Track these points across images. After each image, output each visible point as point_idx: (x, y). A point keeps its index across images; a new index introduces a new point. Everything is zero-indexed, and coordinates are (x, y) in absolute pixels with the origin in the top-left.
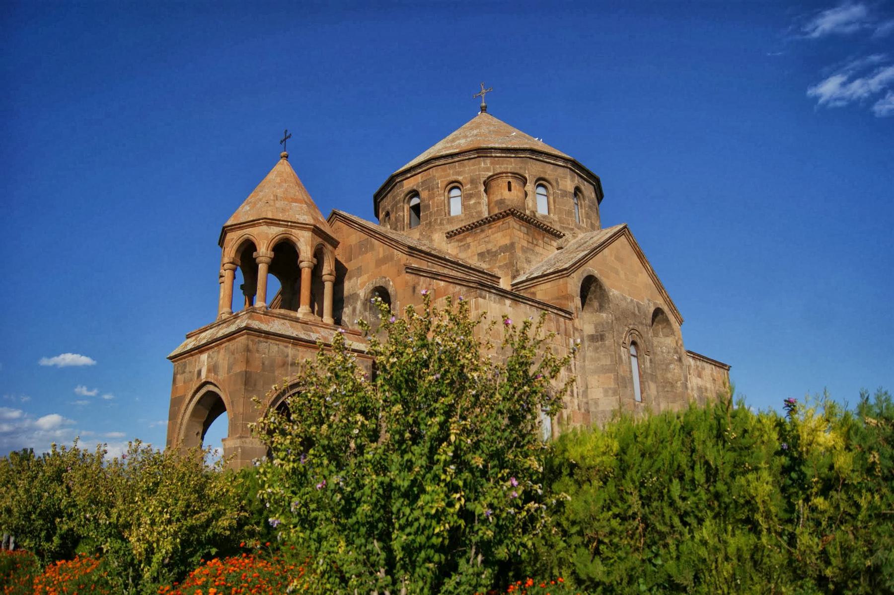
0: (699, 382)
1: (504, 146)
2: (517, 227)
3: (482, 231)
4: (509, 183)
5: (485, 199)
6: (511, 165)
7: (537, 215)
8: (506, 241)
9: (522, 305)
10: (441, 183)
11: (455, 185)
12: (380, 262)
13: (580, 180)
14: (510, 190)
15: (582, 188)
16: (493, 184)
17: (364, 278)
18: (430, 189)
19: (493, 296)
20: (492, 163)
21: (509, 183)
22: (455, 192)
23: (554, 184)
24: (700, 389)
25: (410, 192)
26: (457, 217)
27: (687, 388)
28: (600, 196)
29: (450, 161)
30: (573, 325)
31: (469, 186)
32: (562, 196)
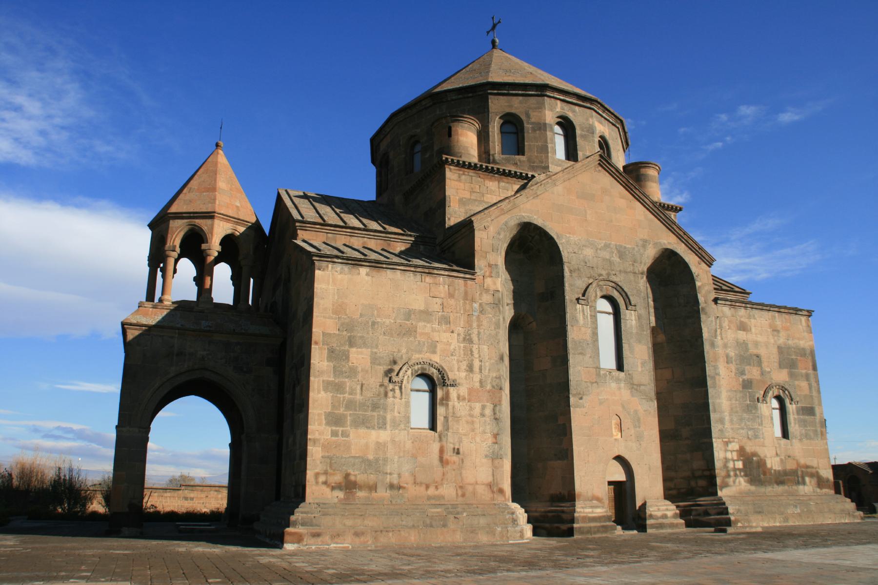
0: (742, 335)
4: (450, 129)
9: (389, 271)
11: (414, 141)
13: (567, 107)
15: (571, 116)
19: (339, 267)
22: (418, 148)
23: (523, 117)
24: (742, 345)
27: (713, 345)
28: (618, 122)
32: (534, 130)
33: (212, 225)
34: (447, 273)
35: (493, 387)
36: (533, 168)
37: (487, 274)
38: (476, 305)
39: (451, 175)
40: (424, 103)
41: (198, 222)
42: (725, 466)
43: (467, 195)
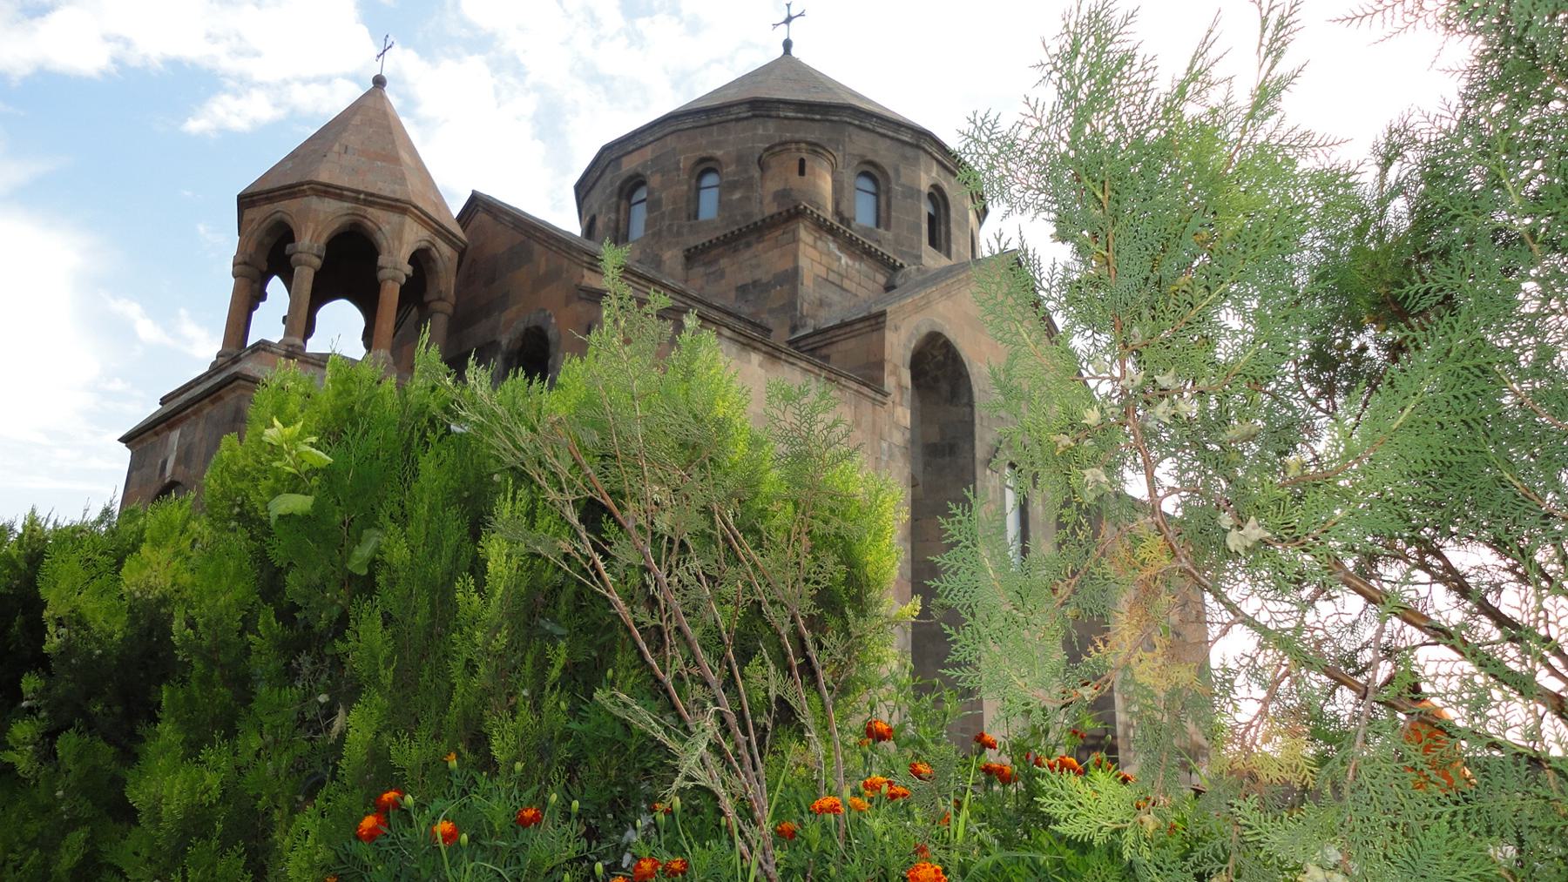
1: (802, 97)
3: (748, 245)
4: (802, 162)
6: (814, 133)
7: (853, 225)
8: (784, 265)
9: (787, 368)
10: (685, 161)
11: (707, 166)
13: (943, 173)
15: (946, 186)
16: (773, 162)
22: (711, 180)
23: (891, 173)
25: (631, 178)
26: (707, 222)
30: (891, 415)
31: (732, 168)
33: (402, 225)
34: (855, 386)
35: (901, 575)
36: (902, 254)
37: (897, 400)
38: (885, 445)
39: (805, 235)
40: (735, 110)
41: (372, 212)
42: (1126, 735)
43: (822, 271)
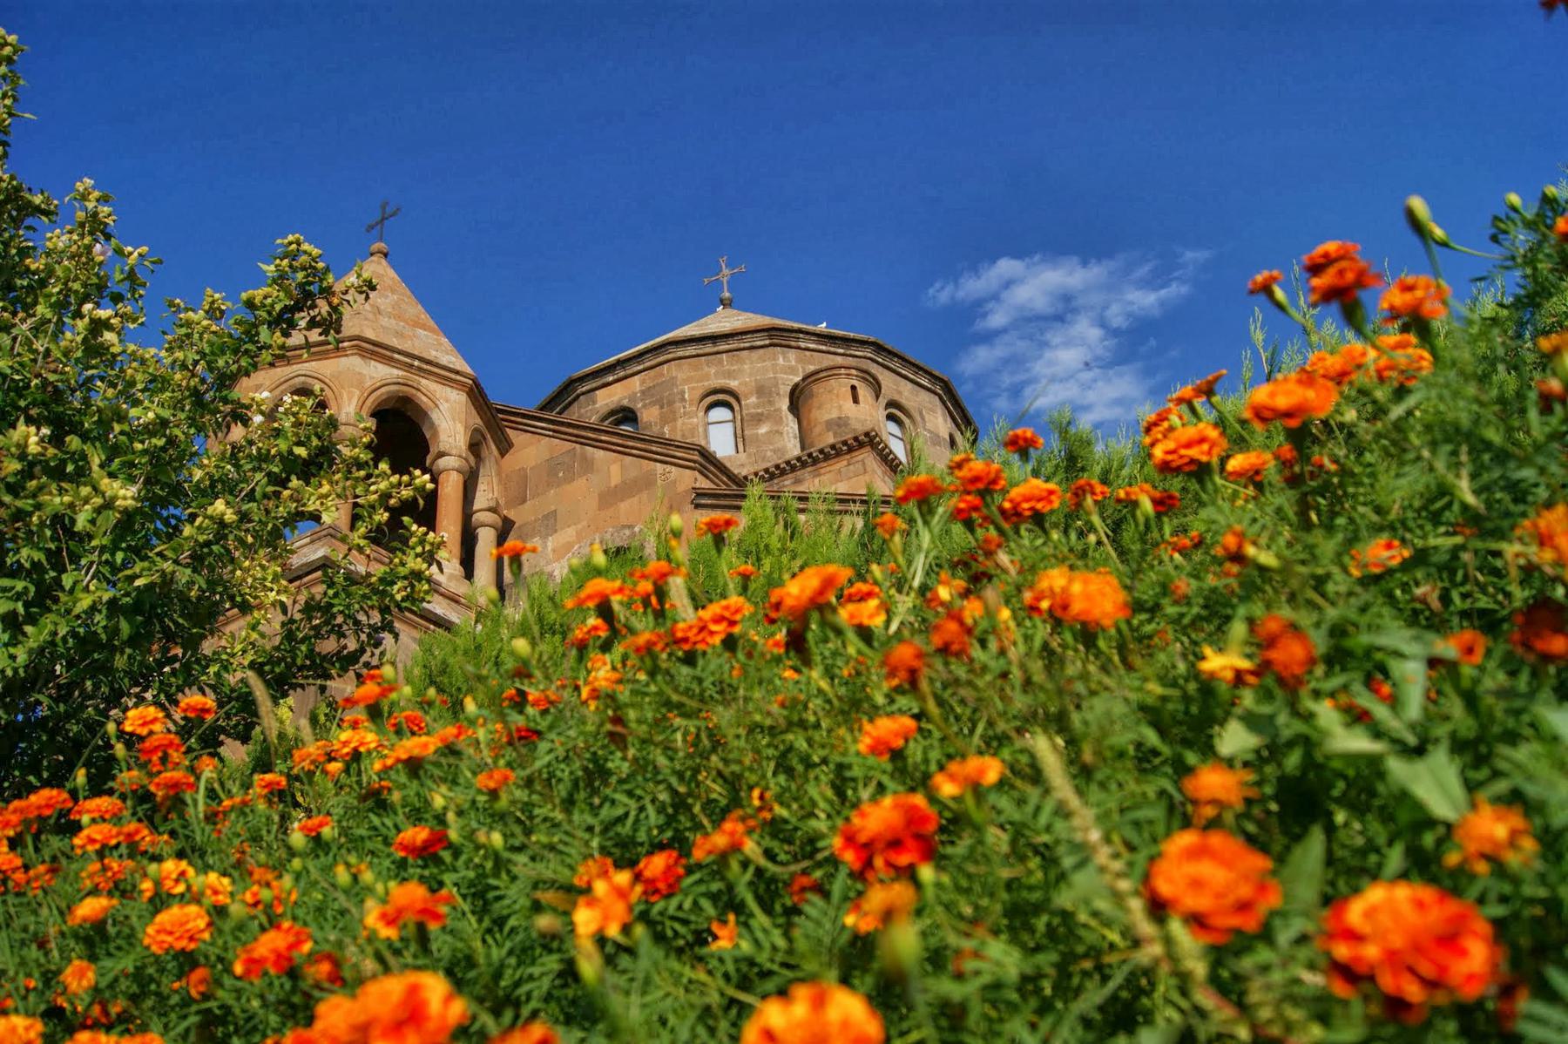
2: (879, 472)
4: (853, 388)
5: (791, 425)
10: (691, 391)
11: (722, 398)
12: (609, 498)
14: (856, 401)
17: (567, 534)
18: (666, 401)
20: (799, 360)
21: (853, 388)
22: (720, 413)
23: (918, 418)
25: (612, 413)
29: (709, 348)
31: (753, 400)
41: (427, 384)
